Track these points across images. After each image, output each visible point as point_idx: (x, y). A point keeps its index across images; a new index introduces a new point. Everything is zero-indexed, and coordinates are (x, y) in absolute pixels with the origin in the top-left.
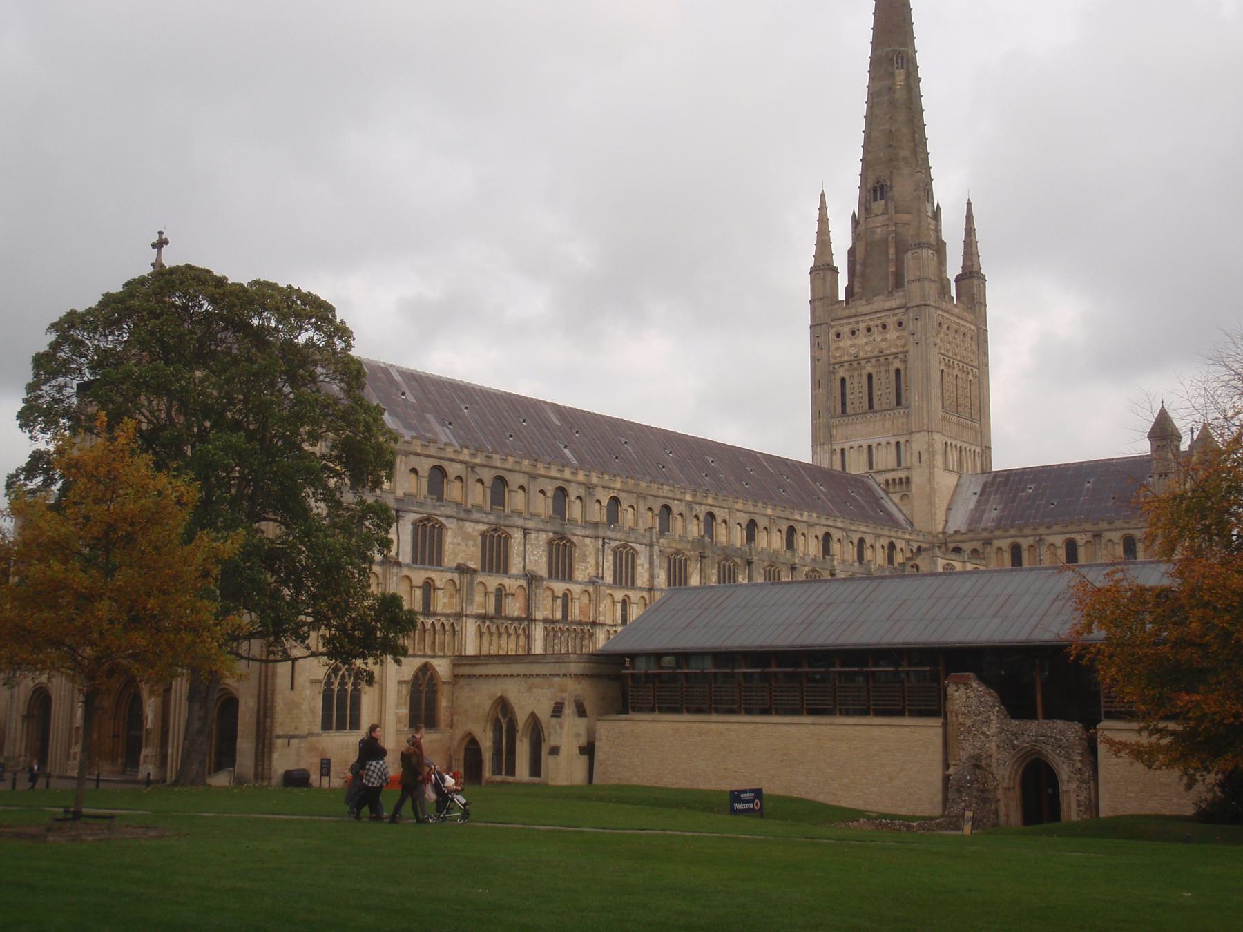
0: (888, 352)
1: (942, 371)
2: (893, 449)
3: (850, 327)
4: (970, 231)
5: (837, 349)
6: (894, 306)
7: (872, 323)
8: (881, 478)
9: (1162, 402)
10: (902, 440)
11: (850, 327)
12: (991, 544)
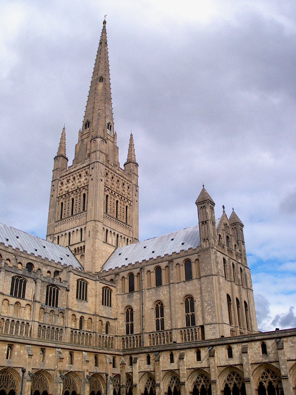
0: (81, 187)
1: (107, 196)
2: (79, 232)
4: (131, 145)
8: (72, 248)
9: (203, 186)
10: (83, 227)
12: (119, 275)
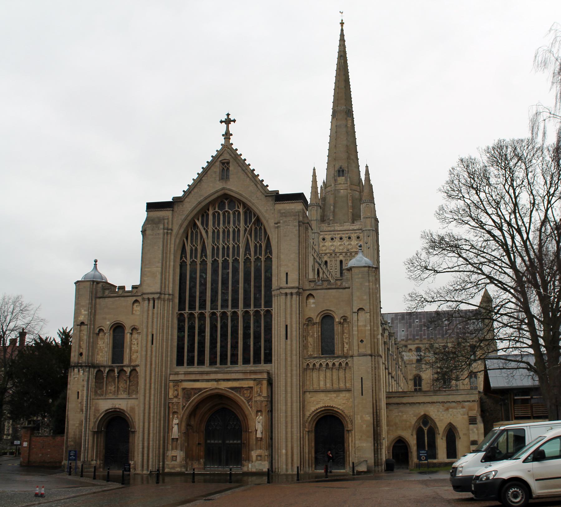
0: (352, 250)
3: (331, 236)
5: (323, 246)
6: (355, 229)
7: (343, 236)
11: (331, 236)
